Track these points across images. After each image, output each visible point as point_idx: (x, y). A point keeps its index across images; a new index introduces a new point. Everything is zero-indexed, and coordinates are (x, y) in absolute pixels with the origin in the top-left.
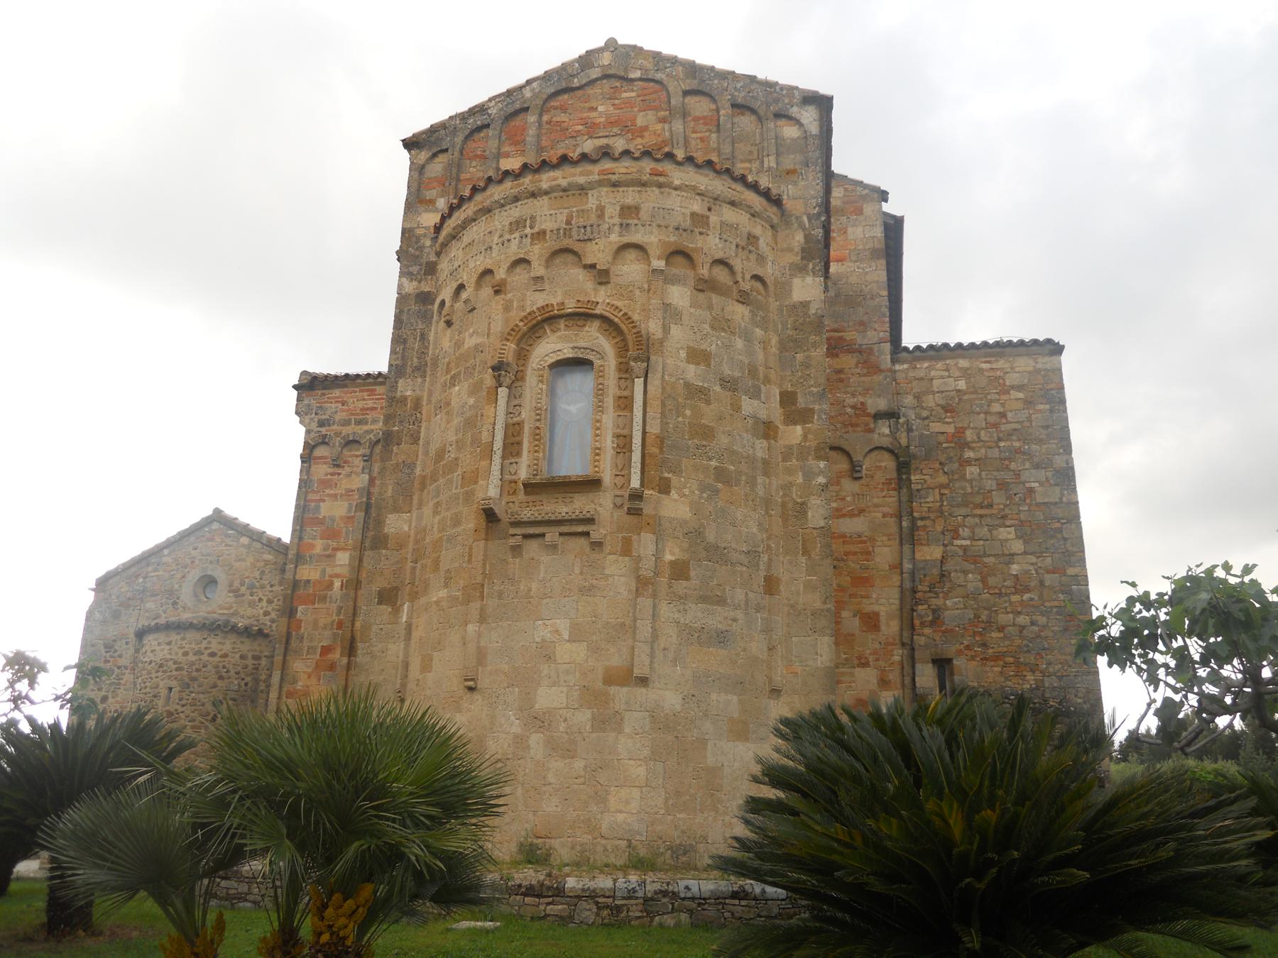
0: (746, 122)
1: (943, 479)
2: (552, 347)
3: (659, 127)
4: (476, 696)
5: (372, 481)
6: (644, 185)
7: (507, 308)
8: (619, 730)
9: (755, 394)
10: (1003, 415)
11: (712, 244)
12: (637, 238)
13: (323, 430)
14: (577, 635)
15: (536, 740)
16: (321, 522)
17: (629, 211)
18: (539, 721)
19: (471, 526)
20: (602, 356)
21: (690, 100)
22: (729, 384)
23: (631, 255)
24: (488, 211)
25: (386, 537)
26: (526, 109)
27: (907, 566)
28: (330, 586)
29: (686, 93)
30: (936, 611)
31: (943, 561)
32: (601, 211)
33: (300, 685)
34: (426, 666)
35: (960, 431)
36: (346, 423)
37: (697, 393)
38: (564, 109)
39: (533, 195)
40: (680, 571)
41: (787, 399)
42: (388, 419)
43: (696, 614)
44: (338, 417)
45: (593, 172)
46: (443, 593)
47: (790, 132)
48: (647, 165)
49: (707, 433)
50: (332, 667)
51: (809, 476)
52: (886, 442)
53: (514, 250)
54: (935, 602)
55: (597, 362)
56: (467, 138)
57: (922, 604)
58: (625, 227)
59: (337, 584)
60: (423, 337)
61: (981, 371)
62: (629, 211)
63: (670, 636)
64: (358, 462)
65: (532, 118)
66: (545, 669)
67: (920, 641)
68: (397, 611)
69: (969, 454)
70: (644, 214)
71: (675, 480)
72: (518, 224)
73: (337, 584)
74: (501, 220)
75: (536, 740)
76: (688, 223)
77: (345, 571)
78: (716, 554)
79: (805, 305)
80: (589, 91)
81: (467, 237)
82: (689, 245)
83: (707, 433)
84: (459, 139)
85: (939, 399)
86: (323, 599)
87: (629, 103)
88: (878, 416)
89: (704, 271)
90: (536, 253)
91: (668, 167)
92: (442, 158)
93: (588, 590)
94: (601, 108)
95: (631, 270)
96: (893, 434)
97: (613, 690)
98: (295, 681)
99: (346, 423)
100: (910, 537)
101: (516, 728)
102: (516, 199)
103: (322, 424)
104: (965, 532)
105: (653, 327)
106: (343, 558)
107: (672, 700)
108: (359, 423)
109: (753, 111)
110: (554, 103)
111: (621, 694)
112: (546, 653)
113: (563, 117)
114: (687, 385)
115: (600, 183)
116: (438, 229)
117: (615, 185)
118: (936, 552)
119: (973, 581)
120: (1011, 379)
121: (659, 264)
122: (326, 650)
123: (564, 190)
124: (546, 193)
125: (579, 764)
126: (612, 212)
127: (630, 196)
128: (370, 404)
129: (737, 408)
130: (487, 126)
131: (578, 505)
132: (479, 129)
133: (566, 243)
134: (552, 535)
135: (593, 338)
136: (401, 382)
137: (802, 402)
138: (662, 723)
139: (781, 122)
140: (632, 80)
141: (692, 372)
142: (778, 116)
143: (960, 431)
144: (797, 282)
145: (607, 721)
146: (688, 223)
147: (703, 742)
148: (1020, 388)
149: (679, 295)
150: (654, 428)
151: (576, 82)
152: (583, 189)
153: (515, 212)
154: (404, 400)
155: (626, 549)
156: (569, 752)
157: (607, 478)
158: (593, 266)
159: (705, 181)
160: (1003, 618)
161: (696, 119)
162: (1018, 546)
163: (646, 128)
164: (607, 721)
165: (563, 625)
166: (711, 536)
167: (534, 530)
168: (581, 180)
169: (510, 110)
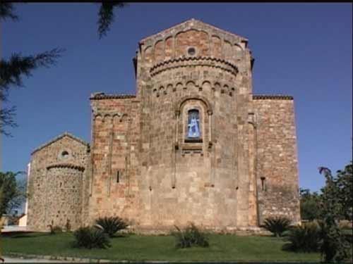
0: (227, 45)
1: (264, 131)
2: (189, 106)
3: (206, 44)
4: (175, 189)
5: (114, 126)
6: (209, 66)
7: (177, 95)
8: (208, 197)
9: (233, 117)
10: (279, 115)
11: (223, 81)
12: (208, 79)
13: (99, 111)
14: (198, 176)
15: (190, 199)
16: (100, 137)
17: (205, 72)
18: (191, 195)
19: (171, 148)
20: (201, 109)
21: (213, 38)
22: (228, 115)
23: (206, 83)
24: (169, 69)
25: (143, 150)
26: (171, 37)
27: (255, 154)
28: (104, 155)
29: (213, 36)
30: (262, 165)
31: (264, 152)
32: (199, 72)
33: (98, 182)
34: (160, 182)
35: (269, 119)
36: (105, 109)
37: (222, 118)
38: (181, 37)
39: (182, 66)
40: (219, 161)
41: (239, 118)
42: (141, 119)
43: (222, 170)
44: (104, 107)
45: (198, 62)
46: (163, 165)
47: (239, 49)
48: (210, 61)
49: (223, 128)
50: (106, 178)
51: (244, 138)
52: (251, 121)
53: (178, 80)
54: (262, 163)
55: (200, 111)
56: (157, 43)
57: (235, 149)
58: (205, 76)
59: (106, 155)
60: (149, 97)
61: (274, 103)
62: (205, 72)
63: (218, 175)
64: (110, 121)
65: (173, 39)
66: (192, 183)
67: (258, 173)
68: (147, 168)
69: (271, 125)
70: (209, 74)
71: (218, 140)
72: (178, 73)
73: (106, 155)
74: (174, 71)
75: (190, 199)
76: (218, 76)
77: (108, 152)
78: (226, 157)
79: (242, 95)
80: (188, 33)
81: (163, 73)
82: (219, 82)
83: (223, 128)
84: (154, 43)
85: (264, 110)
86: (102, 159)
87: (198, 37)
88: (249, 114)
89: (223, 88)
90: (184, 82)
91: (214, 61)
92: (150, 48)
93: (200, 166)
94: (191, 38)
95: (206, 87)
96: (253, 119)
97: (206, 188)
98: (96, 181)
99: (105, 109)
100: (257, 147)
101: (186, 196)
102: (177, 67)
103: (99, 109)
104: (269, 145)
105: (212, 102)
106: (107, 148)
107: (218, 190)
108: (110, 109)
109: (229, 43)
110: (179, 35)
111: (208, 189)
112: (192, 179)
113: (180, 39)
114: (220, 116)
115: (199, 65)
116: (152, 69)
117: (203, 66)
118: (263, 150)
119: (271, 158)
120: (281, 105)
121: (213, 86)
122: (104, 173)
123: (190, 66)
124: (185, 66)
125: (200, 204)
126: (202, 72)
127: (206, 68)
128: (112, 104)
129: (229, 121)
130: (161, 40)
131: (197, 144)
132: (159, 41)
133: (192, 80)
134: (192, 152)
135: (198, 104)
136: (144, 110)
137: (243, 119)
138: (217, 195)
139: (236, 47)
140: (199, 31)
141: (220, 113)
142: (236, 45)
143: (269, 119)
144: (241, 89)
145: (206, 195)
146: (218, 76)
147: (224, 199)
148: (283, 108)
149: (217, 94)
150: (213, 128)
151: (184, 30)
152: (195, 66)
153: (177, 70)
154: (144, 114)
155: (208, 156)
156: (198, 202)
157: (203, 138)
158: (197, 86)
159: (223, 65)
160: (278, 168)
161: (215, 43)
162: (281, 149)
163: (202, 45)
164: (206, 195)
165: (195, 173)
166: (225, 153)
167: (186, 150)
168: (194, 64)
169: (167, 36)
